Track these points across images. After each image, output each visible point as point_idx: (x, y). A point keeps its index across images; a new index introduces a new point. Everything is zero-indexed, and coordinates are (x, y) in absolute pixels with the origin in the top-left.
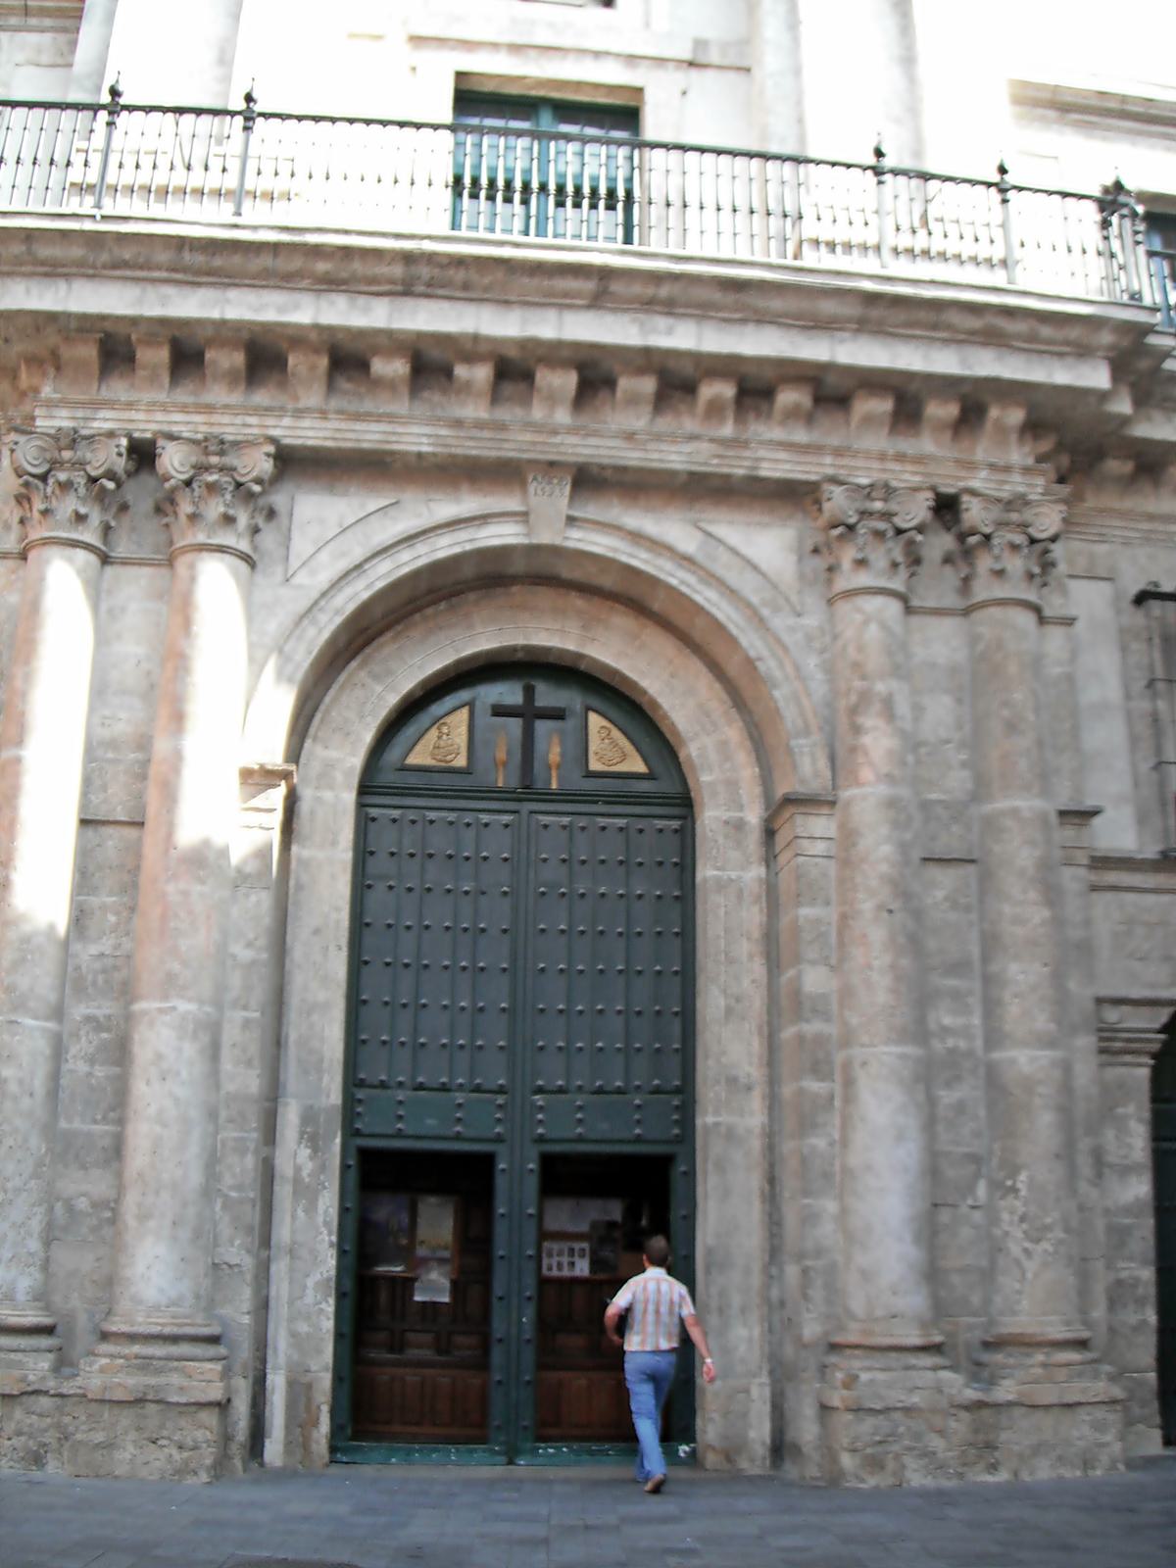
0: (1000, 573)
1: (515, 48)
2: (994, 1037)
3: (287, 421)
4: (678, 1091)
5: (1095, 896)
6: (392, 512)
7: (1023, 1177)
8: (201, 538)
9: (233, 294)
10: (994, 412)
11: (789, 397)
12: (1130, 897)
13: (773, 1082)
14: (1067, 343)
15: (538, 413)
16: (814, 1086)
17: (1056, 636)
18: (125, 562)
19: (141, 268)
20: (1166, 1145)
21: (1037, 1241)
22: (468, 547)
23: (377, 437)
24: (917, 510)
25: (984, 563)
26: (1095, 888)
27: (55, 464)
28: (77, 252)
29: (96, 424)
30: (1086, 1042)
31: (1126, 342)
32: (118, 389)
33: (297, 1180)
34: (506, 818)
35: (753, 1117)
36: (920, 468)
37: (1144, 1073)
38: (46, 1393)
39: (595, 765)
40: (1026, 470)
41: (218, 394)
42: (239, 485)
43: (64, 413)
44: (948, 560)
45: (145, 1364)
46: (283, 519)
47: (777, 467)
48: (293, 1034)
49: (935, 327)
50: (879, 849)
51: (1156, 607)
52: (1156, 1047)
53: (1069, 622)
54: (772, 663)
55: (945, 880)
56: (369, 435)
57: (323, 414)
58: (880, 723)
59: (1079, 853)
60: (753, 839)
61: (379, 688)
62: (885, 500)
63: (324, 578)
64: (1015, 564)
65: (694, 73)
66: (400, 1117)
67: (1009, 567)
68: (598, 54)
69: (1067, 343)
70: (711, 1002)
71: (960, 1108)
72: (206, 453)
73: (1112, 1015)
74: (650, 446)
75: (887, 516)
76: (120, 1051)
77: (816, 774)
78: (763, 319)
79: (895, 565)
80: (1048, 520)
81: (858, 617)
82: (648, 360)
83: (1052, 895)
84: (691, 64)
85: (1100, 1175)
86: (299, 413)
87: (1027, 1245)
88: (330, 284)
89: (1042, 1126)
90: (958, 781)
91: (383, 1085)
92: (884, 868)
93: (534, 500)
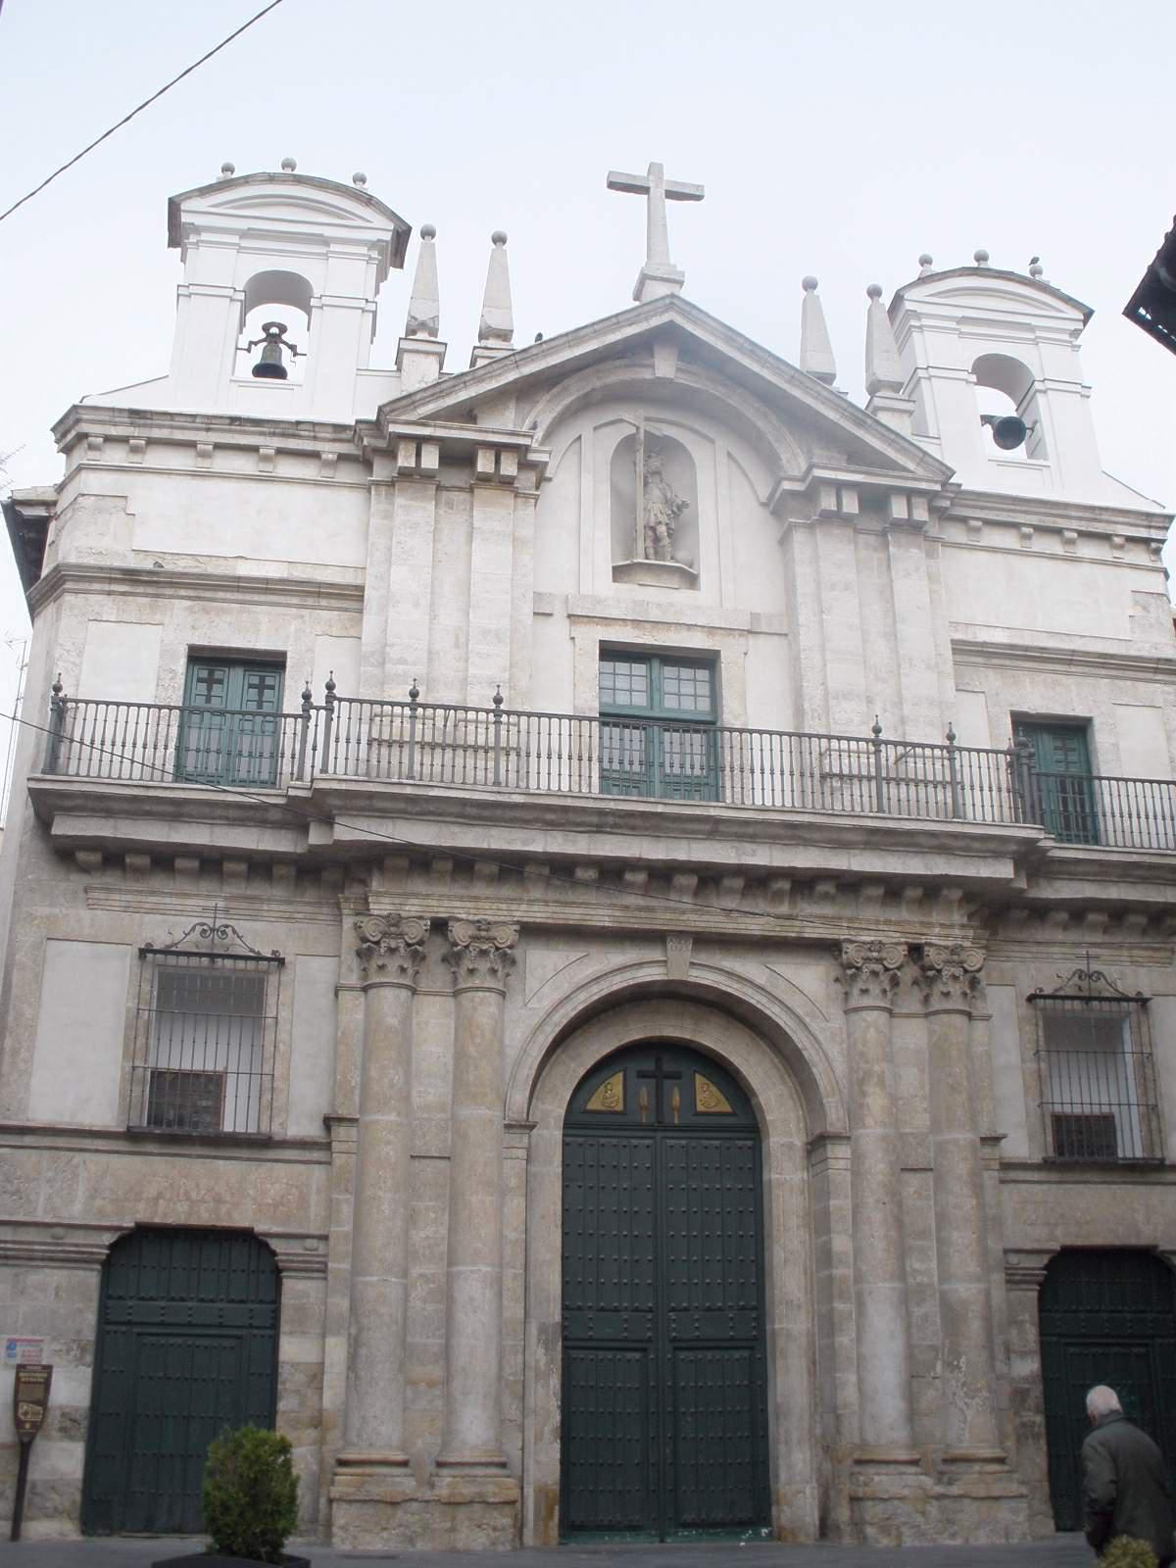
0: (947, 995)
2: (945, 1276)
3: (524, 907)
4: (755, 1308)
5: (1003, 1186)
6: (585, 960)
7: (963, 1359)
8: (477, 982)
9: (494, 831)
10: (945, 892)
11: (821, 888)
12: (1023, 1186)
14: (988, 851)
17: (980, 1026)
18: (427, 994)
19: (440, 815)
20: (1048, 1339)
21: (973, 1398)
22: (631, 982)
23: (577, 917)
24: (896, 956)
25: (939, 987)
26: (1002, 1182)
27: (385, 934)
28: (401, 805)
29: (407, 908)
30: (998, 1277)
31: (1023, 849)
32: (419, 885)
33: (537, 1369)
34: (647, 1142)
36: (900, 929)
37: (1035, 1294)
38: (416, 1500)
39: (700, 1108)
40: (963, 926)
41: (480, 889)
42: (497, 949)
43: (387, 900)
44: (915, 982)
46: (520, 964)
47: (813, 932)
49: (909, 845)
50: (878, 1166)
51: (1041, 1002)
52: (1041, 1278)
53: (987, 1018)
54: (813, 1052)
55: (914, 1181)
56: (573, 915)
57: (546, 903)
58: (878, 1090)
59: (992, 1163)
60: (799, 1155)
61: (573, 1065)
62: (878, 952)
63: (546, 1004)
64: (956, 989)
65: (751, 639)
66: (591, 1328)
67: (951, 990)
68: (690, 627)
69: (988, 851)
71: (926, 1318)
72: (479, 929)
73: (1014, 1259)
74: (740, 920)
75: (879, 961)
77: (838, 1120)
78: (808, 843)
79: (884, 991)
80: (975, 959)
81: (864, 1024)
82: (739, 871)
83: (978, 1189)
84: (750, 632)
85: (1009, 1359)
86: (531, 902)
87: (967, 1400)
88: (552, 825)
89: (975, 1326)
90: (921, 1121)
91: (579, 1308)
92: (880, 1177)
93: (669, 952)
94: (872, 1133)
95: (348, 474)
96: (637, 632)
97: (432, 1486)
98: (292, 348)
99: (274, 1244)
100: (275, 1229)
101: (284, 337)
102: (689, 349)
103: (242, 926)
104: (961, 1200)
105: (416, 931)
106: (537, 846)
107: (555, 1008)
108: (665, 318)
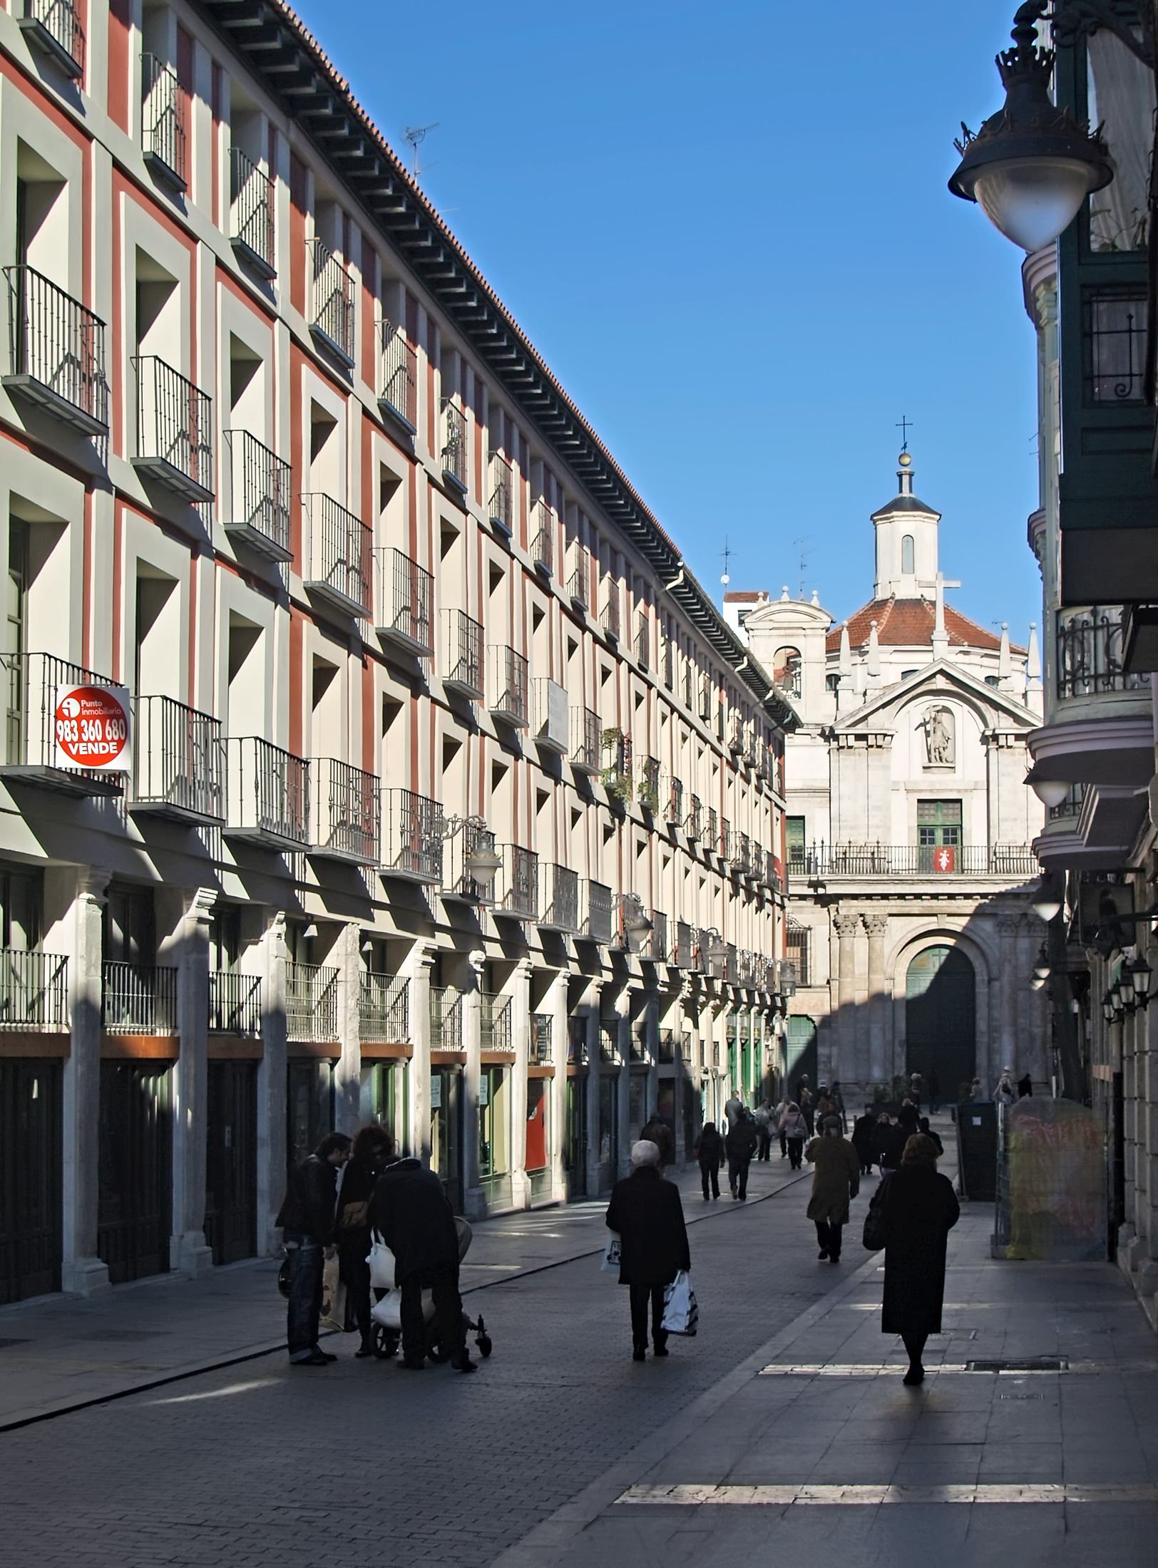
1: (931, 791)
50: (1007, 989)
63: (897, 939)
68: (951, 790)
70: (978, 1016)
89: (1038, 1043)
94: (1006, 979)
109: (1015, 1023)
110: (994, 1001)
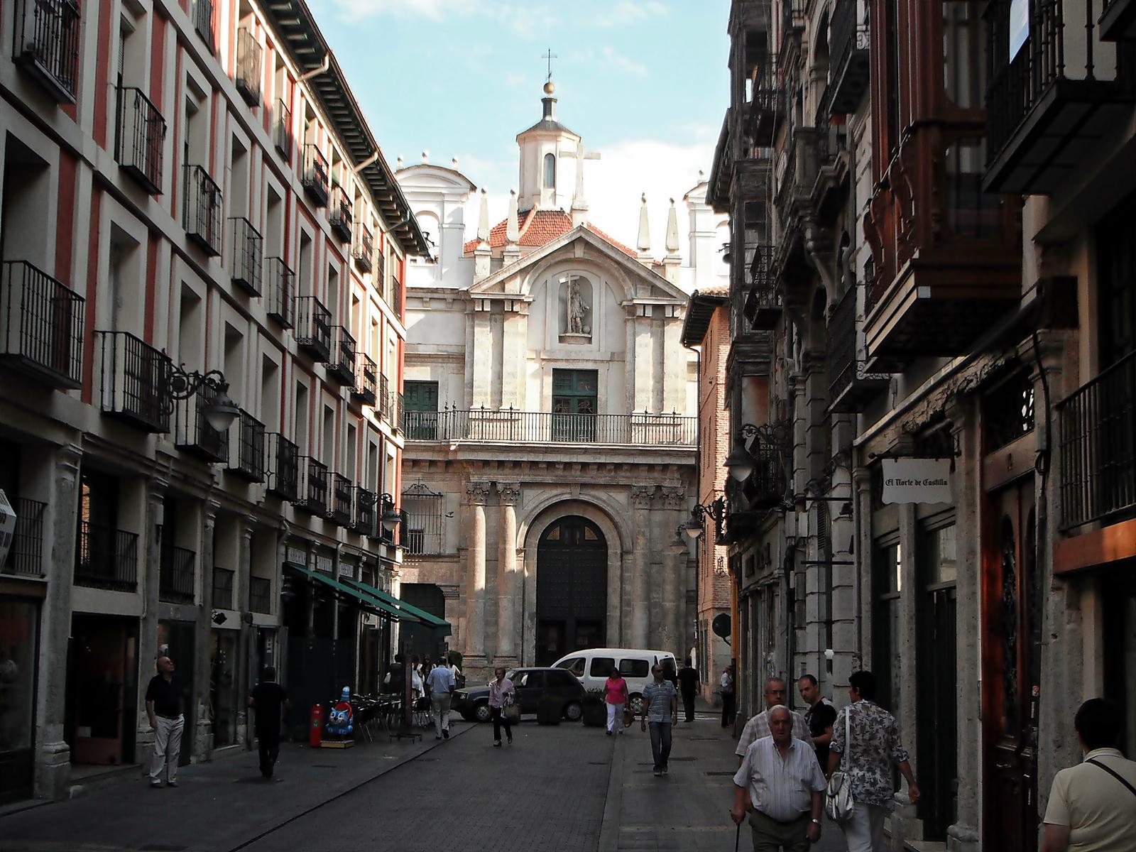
1: (567, 360)
13: (621, 606)
15: (573, 472)
16: (629, 609)
25: (667, 502)
35: (618, 614)
39: (586, 539)
41: (507, 471)
45: (505, 661)
47: (622, 482)
48: (526, 598)
50: (640, 563)
56: (539, 479)
70: (610, 590)
76: (496, 604)
89: (671, 618)
94: (639, 552)
95: (457, 306)
96: (566, 364)
97: (492, 663)
98: (433, 243)
99: (442, 588)
100: (443, 584)
101: (429, 238)
102: (588, 244)
103: (428, 484)
104: (669, 575)
105: (487, 487)
106: (525, 459)
107: (533, 510)
108: (578, 235)
109: (648, 598)
110: (627, 574)
